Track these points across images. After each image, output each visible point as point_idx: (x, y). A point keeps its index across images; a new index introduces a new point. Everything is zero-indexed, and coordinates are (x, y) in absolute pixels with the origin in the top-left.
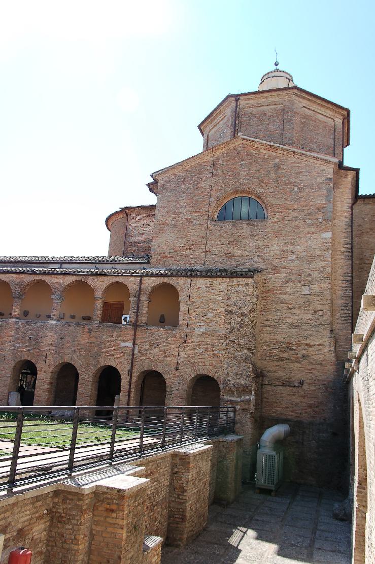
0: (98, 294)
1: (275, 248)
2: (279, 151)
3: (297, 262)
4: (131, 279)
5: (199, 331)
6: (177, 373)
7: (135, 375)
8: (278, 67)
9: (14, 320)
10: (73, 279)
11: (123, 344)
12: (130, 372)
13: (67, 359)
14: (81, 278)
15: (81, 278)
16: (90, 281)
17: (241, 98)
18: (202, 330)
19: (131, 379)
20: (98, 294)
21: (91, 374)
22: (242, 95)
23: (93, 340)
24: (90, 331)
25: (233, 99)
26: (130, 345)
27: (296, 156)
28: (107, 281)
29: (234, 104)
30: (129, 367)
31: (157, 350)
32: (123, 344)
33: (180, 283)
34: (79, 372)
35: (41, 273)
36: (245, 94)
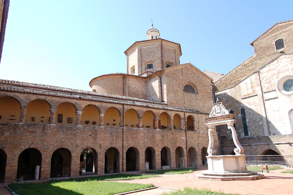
0: (172, 118)
1: (201, 104)
2: (198, 72)
3: (207, 110)
4: (181, 113)
5: (201, 132)
6: (198, 147)
7: (188, 149)
8: (153, 27)
9: (142, 129)
10: (163, 111)
11: (183, 138)
12: (186, 148)
13: (166, 145)
14: (166, 111)
15: (166, 111)
16: (169, 113)
17: (163, 41)
18: (202, 132)
19: (187, 151)
20: (172, 118)
21: (175, 150)
22: (164, 40)
23: (174, 137)
24: (172, 134)
25: (161, 40)
26: (184, 138)
27: (203, 75)
28: (174, 113)
29: (160, 42)
30: (186, 146)
31: (192, 140)
32: (183, 138)
33: (195, 116)
34: (171, 150)
35: (152, 108)
36: (165, 40)
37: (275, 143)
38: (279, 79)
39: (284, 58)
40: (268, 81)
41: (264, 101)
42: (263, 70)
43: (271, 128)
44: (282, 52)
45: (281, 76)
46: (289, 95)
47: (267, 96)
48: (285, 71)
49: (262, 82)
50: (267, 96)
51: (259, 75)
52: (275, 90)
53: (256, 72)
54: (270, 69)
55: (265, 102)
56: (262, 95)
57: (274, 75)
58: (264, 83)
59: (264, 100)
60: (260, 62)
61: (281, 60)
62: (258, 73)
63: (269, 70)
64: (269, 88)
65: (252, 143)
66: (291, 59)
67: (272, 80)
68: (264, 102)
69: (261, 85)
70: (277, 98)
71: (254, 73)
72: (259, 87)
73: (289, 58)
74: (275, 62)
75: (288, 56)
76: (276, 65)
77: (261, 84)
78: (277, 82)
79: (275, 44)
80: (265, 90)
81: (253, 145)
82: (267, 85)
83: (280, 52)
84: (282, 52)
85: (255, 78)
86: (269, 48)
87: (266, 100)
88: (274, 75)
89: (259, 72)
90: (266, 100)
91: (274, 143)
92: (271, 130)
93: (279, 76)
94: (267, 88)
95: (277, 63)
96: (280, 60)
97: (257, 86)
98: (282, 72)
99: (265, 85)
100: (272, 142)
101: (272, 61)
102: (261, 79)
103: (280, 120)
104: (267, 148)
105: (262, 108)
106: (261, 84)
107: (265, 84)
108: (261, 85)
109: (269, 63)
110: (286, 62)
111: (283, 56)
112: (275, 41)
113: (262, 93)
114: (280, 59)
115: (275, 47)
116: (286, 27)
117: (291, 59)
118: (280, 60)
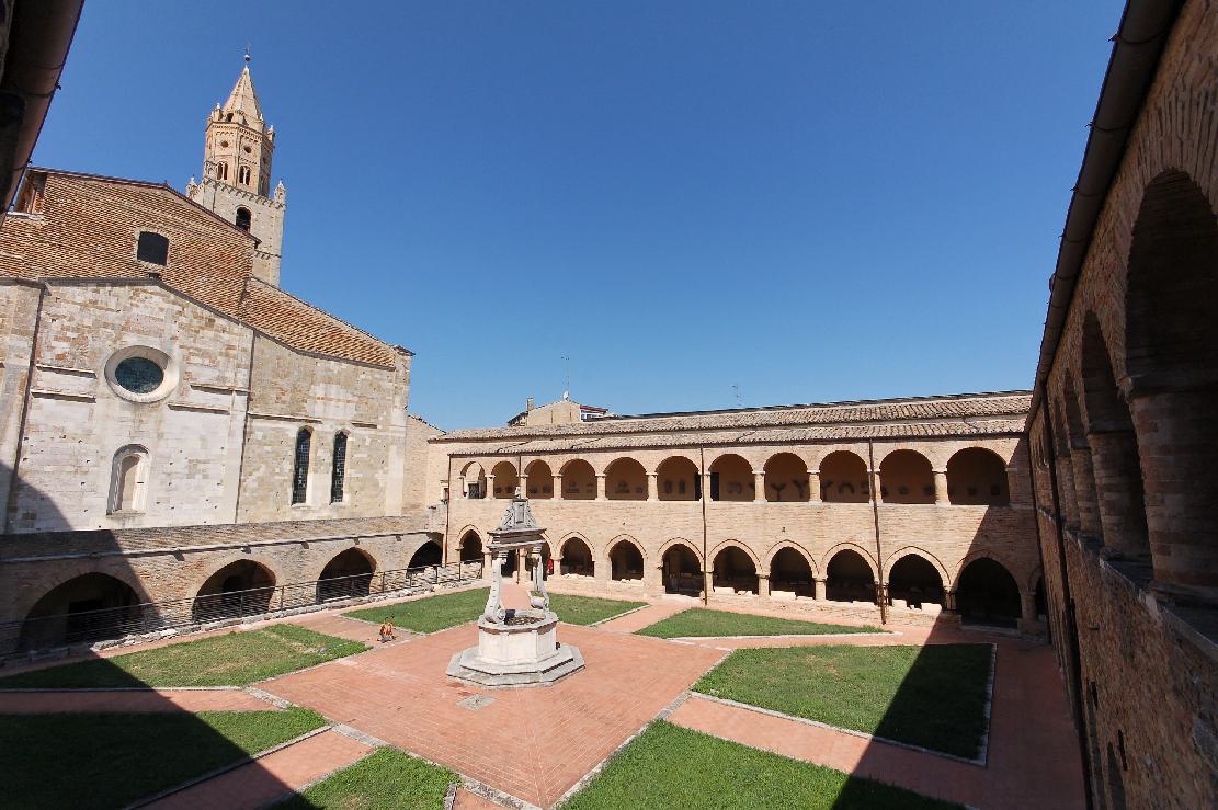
37: (129, 552)
38: (118, 346)
39: (157, 294)
40: (69, 334)
41: (31, 396)
42: (63, 289)
43: (22, 494)
44: (156, 278)
45: (131, 340)
46: (135, 403)
47: (45, 381)
48: (148, 333)
49: (46, 327)
50: (45, 381)
51: (41, 298)
52: (93, 376)
53: (32, 285)
54: (96, 302)
55: (34, 401)
56: (26, 371)
57: (106, 325)
58: (52, 335)
59: (32, 390)
60: (59, 260)
61: (147, 295)
62: (37, 291)
63: (90, 302)
64: (69, 358)
65: (17, 554)
66: (179, 308)
67: (90, 338)
68: (26, 400)
69: (35, 337)
70: (93, 400)
71: (18, 282)
72: (26, 344)
73: (174, 303)
74: (124, 292)
75: (172, 297)
76: (125, 301)
77: (36, 332)
78: (111, 352)
79: (137, 237)
80: (47, 358)
81: (16, 563)
82: (62, 347)
83: (151, 274)
84: (157, 276)
85: (14, 300)
86: (112, 234)
87: (37, 395)
88: (106, 325)
89: (42, 288)
90: (37, 395)
91: (125, 552)
92: (22, 501)
93: (125, 338)
94: (60, 357)
95: (131, 298)
96: (142, 295)
97: (21, 333)
98: (138, 331)
99: (54, 343)
100: (119, 549)
101: (116, 283)
102: (43, 314)
103: (76, 472)
104: (86, 569)
105: (9, 416)
106: (36, 332)
107: (56, 339)
108: (35, 337)
109: (101, 283)
110: (162, 310)
111: (157, 288)
112: (144, 229)
113: (32, 363)
114: (145, 291)
115: (136, 246)
116: (189, 216)
117: (179, 308)
118: (142, 295)
